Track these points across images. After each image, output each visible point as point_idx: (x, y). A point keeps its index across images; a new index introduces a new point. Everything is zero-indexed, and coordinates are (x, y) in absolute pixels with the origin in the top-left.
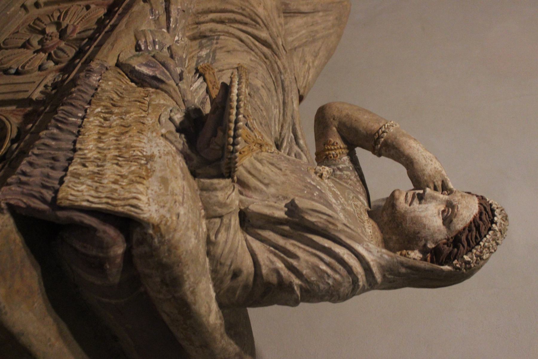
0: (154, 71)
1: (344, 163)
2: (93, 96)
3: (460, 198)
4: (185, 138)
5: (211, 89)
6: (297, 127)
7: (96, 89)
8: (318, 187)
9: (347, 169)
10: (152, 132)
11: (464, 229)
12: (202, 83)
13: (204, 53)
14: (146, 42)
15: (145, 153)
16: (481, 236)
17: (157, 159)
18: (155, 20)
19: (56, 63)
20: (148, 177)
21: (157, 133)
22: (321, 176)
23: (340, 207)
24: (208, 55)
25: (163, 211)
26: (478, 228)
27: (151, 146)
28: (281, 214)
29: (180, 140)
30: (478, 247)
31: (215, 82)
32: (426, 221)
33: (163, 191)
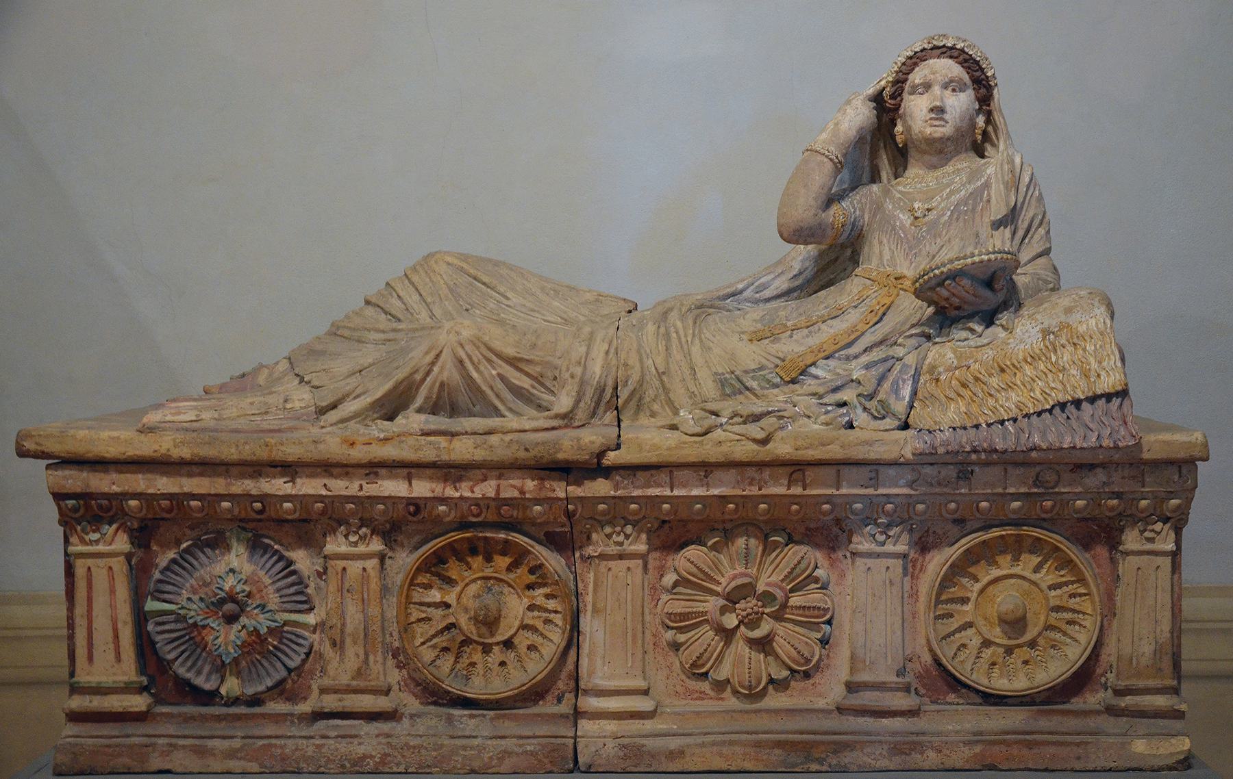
0: (904, 381)
1: (848, 206)
2: (965, 428)
3: (938, 75)
4: (1001, 312)
5: (826, 353)
6: (721, 293)
7: (954, 429)
8: (952, 208)
9: (852, 203)
10: (1008, 344)
11: (968, 73)
12: (817, 368)
13: (754, 384)
14: (840, 416)
15: (1040, 340)
16: (969, 60)
17: (1046, 325)
18: (793, 421)
19: (817, 567)
20: (1069, 325)
21: (1009, 339)
22: (929, 210)
23: (968, 186)
24: (753, 378)
25: (1096, 304)
26: (966, 61)
27: (1029, 337)
28: (1008, 232)
29: (1004, 318)
30: (981, 63)
31: (812, 352)
32: (965, 107)
33: (1078, 309)
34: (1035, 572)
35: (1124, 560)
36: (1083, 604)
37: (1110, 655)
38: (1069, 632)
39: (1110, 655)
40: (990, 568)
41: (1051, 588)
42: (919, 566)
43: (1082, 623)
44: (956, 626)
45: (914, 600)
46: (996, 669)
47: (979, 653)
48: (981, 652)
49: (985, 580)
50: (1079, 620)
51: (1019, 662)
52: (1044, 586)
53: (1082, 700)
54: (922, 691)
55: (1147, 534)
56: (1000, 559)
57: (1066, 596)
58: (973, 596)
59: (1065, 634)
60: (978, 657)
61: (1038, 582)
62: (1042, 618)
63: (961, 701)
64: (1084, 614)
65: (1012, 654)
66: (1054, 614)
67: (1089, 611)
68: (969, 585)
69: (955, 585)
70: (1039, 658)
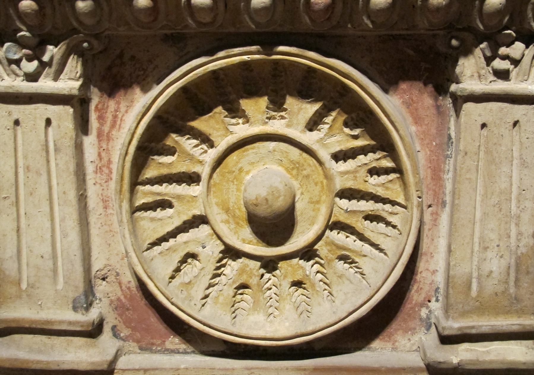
34: (311, 130)
35: (458, 112)
36: (390, 185)
37: (434, 272)
38: (368, 234)
39: (434, 272)
40: (234, 121)
41: (338, 157)
42: (109, 117)
43: (390, 219)
44: (177, 222)
45: (104, 177)
46: (248, 296)
47: (218, 268)
48: (224, 266)
49: (222, 145)
50: (384, 215)
51: (286, 284)
52: (325, 155)
53: (389, 345)
54: (125, 332)
55: (498, 64)
56: (246, 104)
57: (363, 172)
58: (204, 171)
59: (362, 238)
60: (219, 275)
61: (315, 147)
62: (324, 211)
63: (190, 349)
64: (393, 203)
65: (275, 269)
66: (344, 203)
67: (401, 199)
68: (197, 152)
69: (171, 152)
70: (319, 276)
